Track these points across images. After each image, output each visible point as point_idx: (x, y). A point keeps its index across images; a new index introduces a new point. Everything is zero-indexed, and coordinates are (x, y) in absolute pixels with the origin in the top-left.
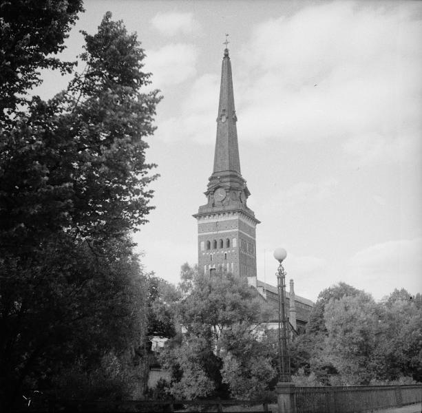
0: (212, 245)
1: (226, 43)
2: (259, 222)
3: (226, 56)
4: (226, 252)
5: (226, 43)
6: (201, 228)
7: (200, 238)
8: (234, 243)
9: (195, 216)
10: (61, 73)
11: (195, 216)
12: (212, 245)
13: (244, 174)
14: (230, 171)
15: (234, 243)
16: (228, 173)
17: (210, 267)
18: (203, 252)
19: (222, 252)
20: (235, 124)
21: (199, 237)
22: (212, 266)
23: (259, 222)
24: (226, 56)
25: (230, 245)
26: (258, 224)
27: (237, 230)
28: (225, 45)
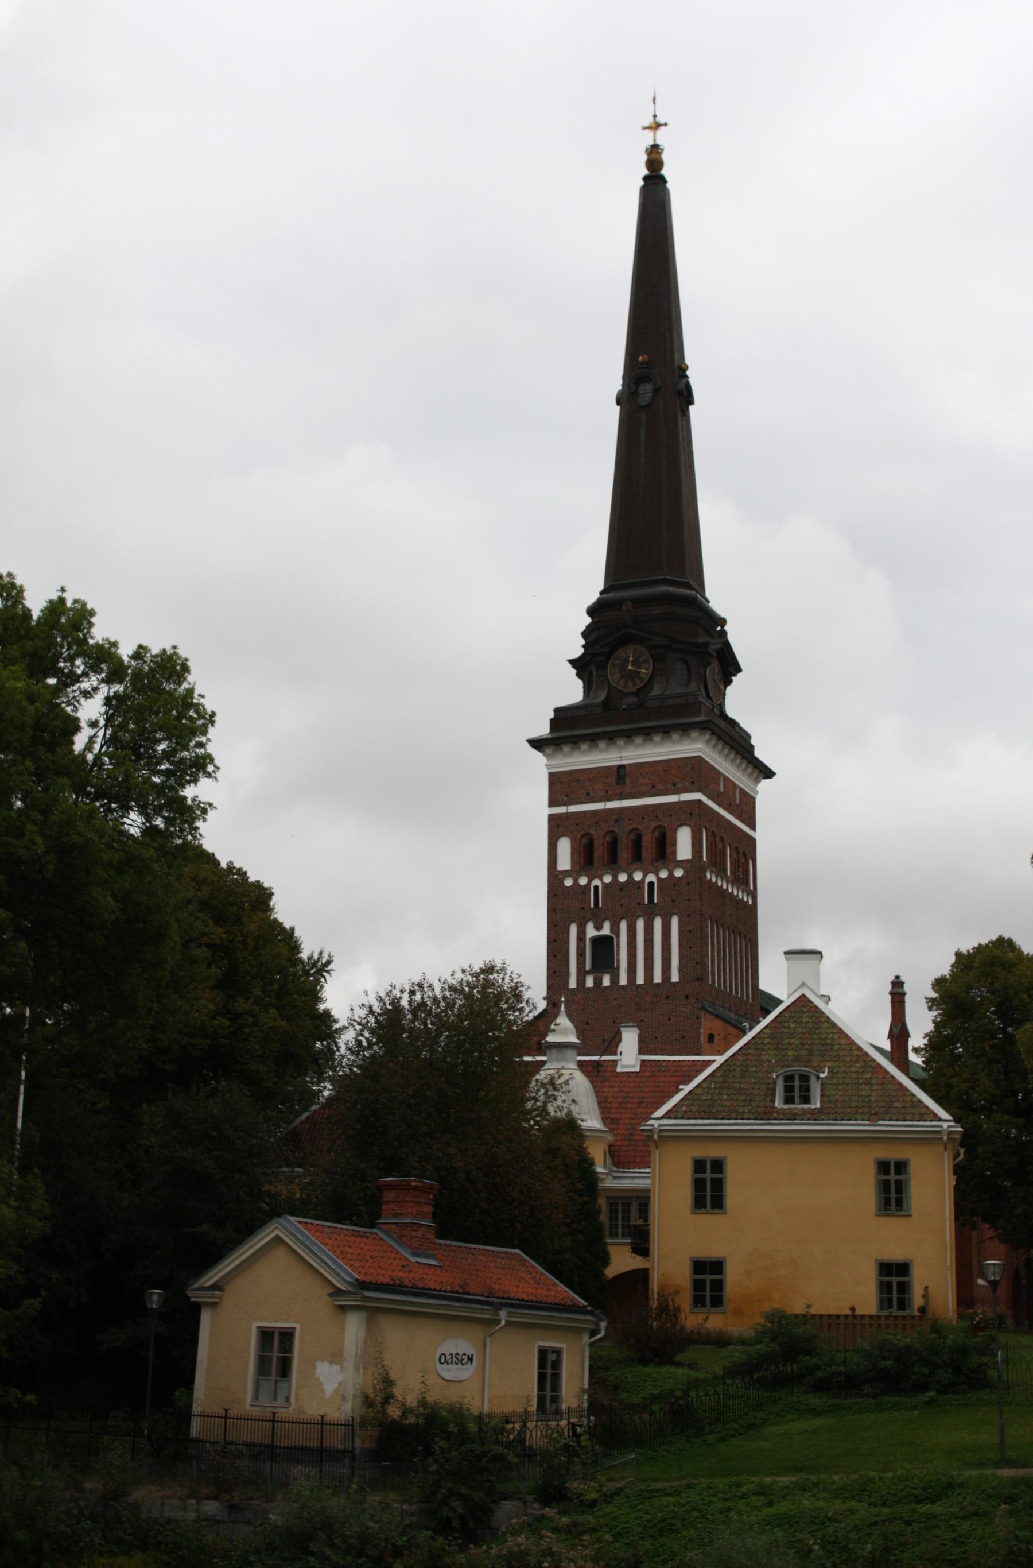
0: (600, 851)
2: (769, 774)
3: (654, 159)
4: (651, 878)
5: (656, 126)
7: (557, 827)
9: (537, 744)
11: (537, 744)
12: (600, 851)
17: (591, 932)
18: (566, 874)
20: (686, 414)
21: (552, 818)
22: (598, 927)
23: (769, 774)
24: (654, 159)
25: (668, 851)
26: (765, 783)
28: (649, 134)
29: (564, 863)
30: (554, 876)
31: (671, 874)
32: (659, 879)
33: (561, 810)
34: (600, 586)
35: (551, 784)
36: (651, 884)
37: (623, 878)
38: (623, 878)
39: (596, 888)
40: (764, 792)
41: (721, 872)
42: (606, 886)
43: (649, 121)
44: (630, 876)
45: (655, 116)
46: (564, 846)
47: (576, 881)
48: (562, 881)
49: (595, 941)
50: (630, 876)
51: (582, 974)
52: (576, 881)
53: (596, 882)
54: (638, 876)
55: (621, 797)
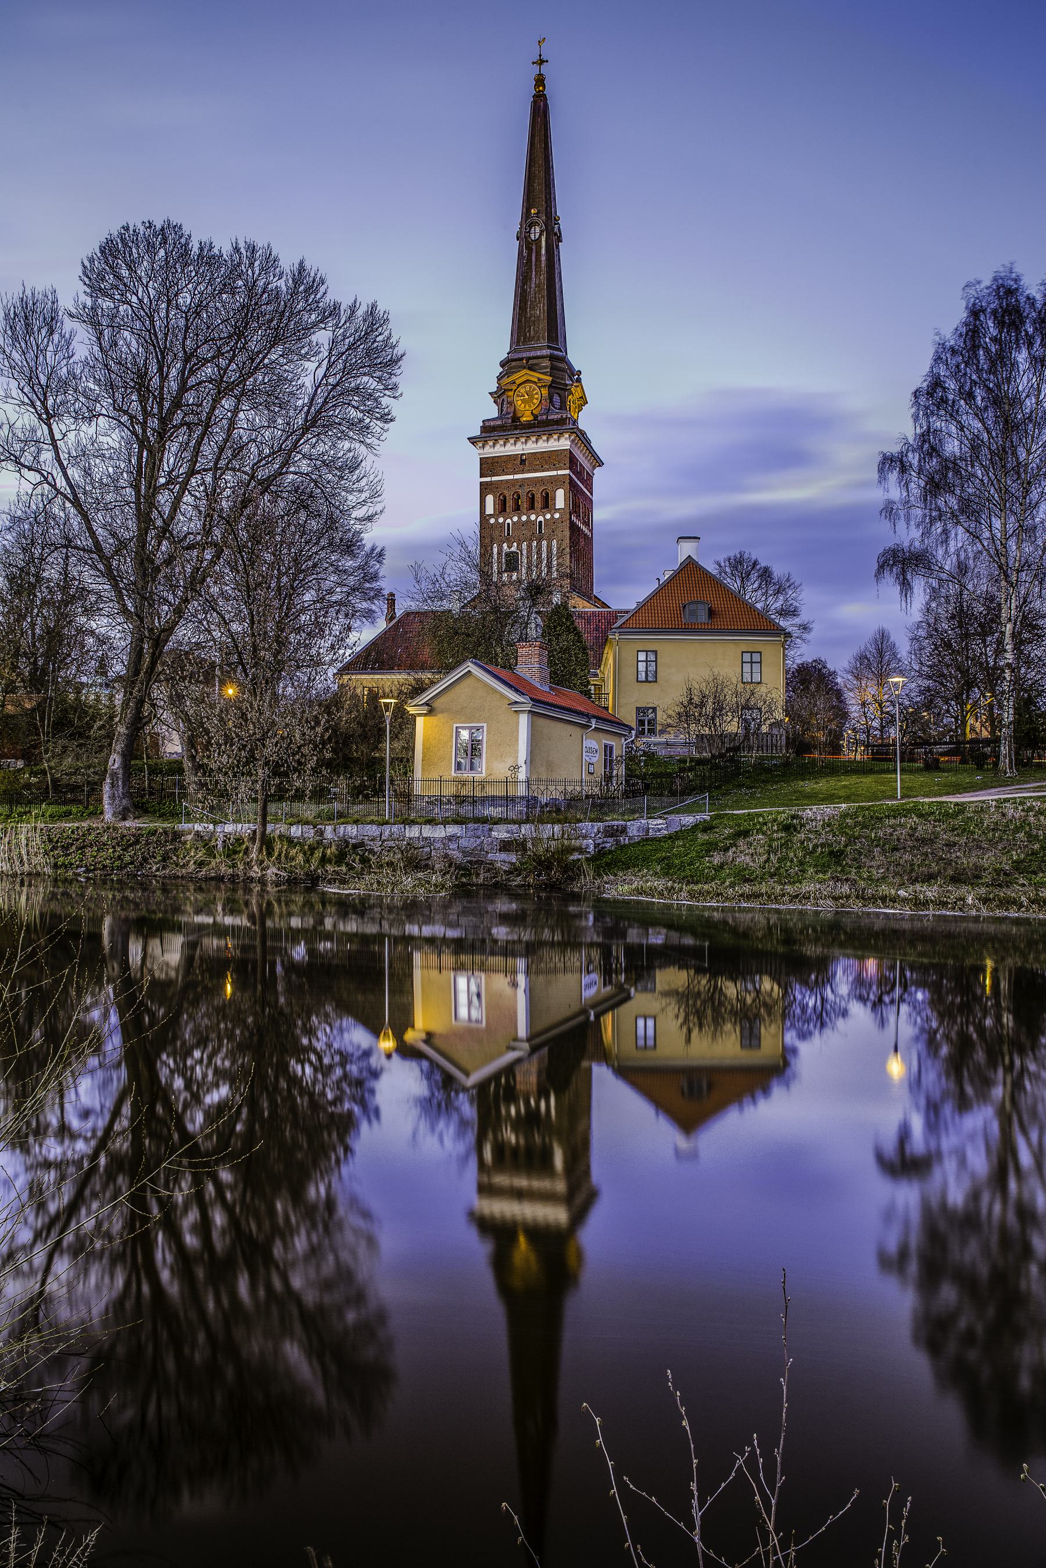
0: (510, 503)
1: (541, 62)
3: (540, 81)
4: (541, 518)
5: (541, 62)
6: (488, 466)
8: (560, 499)
9: (473, 440)
10: (146, 221)
11: (473, 440)
12: (510, 503)
13: (576, 356)
14: (549, 347)
15: (560, 499)
16: (546, 352)
19: (533, 517)
22: (510, 547)
24: (540, 81)
27: (567, 472)
28: (536, 67)
29: (490, 510)
30: (484, 517)
31: (552, 516)
32: (545, 519)
33: (488, 479)
34: (508, 350)
35: (481, 464)
36: (540, 522)
37: (524, 518)
38: (524, 518)
39: (509, 524)
40: (598, 474)
41: (578, 517)
42: (514, 523)
43: (536, 58)
44: (528, 517)
45: (540, 55)
46: (490, 499)
47: (497, 520)
48: (488, 520)
49: (507, 555)
50: (528, 517)
51: (500, 573)
52: (497, 520)
53: (509, 521)
54: (533, 517)
55: (523, 472)
